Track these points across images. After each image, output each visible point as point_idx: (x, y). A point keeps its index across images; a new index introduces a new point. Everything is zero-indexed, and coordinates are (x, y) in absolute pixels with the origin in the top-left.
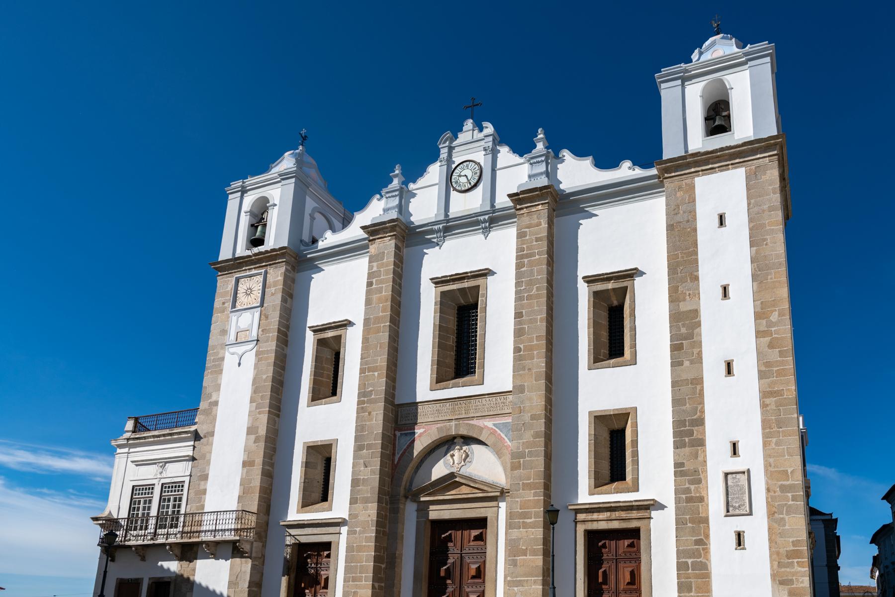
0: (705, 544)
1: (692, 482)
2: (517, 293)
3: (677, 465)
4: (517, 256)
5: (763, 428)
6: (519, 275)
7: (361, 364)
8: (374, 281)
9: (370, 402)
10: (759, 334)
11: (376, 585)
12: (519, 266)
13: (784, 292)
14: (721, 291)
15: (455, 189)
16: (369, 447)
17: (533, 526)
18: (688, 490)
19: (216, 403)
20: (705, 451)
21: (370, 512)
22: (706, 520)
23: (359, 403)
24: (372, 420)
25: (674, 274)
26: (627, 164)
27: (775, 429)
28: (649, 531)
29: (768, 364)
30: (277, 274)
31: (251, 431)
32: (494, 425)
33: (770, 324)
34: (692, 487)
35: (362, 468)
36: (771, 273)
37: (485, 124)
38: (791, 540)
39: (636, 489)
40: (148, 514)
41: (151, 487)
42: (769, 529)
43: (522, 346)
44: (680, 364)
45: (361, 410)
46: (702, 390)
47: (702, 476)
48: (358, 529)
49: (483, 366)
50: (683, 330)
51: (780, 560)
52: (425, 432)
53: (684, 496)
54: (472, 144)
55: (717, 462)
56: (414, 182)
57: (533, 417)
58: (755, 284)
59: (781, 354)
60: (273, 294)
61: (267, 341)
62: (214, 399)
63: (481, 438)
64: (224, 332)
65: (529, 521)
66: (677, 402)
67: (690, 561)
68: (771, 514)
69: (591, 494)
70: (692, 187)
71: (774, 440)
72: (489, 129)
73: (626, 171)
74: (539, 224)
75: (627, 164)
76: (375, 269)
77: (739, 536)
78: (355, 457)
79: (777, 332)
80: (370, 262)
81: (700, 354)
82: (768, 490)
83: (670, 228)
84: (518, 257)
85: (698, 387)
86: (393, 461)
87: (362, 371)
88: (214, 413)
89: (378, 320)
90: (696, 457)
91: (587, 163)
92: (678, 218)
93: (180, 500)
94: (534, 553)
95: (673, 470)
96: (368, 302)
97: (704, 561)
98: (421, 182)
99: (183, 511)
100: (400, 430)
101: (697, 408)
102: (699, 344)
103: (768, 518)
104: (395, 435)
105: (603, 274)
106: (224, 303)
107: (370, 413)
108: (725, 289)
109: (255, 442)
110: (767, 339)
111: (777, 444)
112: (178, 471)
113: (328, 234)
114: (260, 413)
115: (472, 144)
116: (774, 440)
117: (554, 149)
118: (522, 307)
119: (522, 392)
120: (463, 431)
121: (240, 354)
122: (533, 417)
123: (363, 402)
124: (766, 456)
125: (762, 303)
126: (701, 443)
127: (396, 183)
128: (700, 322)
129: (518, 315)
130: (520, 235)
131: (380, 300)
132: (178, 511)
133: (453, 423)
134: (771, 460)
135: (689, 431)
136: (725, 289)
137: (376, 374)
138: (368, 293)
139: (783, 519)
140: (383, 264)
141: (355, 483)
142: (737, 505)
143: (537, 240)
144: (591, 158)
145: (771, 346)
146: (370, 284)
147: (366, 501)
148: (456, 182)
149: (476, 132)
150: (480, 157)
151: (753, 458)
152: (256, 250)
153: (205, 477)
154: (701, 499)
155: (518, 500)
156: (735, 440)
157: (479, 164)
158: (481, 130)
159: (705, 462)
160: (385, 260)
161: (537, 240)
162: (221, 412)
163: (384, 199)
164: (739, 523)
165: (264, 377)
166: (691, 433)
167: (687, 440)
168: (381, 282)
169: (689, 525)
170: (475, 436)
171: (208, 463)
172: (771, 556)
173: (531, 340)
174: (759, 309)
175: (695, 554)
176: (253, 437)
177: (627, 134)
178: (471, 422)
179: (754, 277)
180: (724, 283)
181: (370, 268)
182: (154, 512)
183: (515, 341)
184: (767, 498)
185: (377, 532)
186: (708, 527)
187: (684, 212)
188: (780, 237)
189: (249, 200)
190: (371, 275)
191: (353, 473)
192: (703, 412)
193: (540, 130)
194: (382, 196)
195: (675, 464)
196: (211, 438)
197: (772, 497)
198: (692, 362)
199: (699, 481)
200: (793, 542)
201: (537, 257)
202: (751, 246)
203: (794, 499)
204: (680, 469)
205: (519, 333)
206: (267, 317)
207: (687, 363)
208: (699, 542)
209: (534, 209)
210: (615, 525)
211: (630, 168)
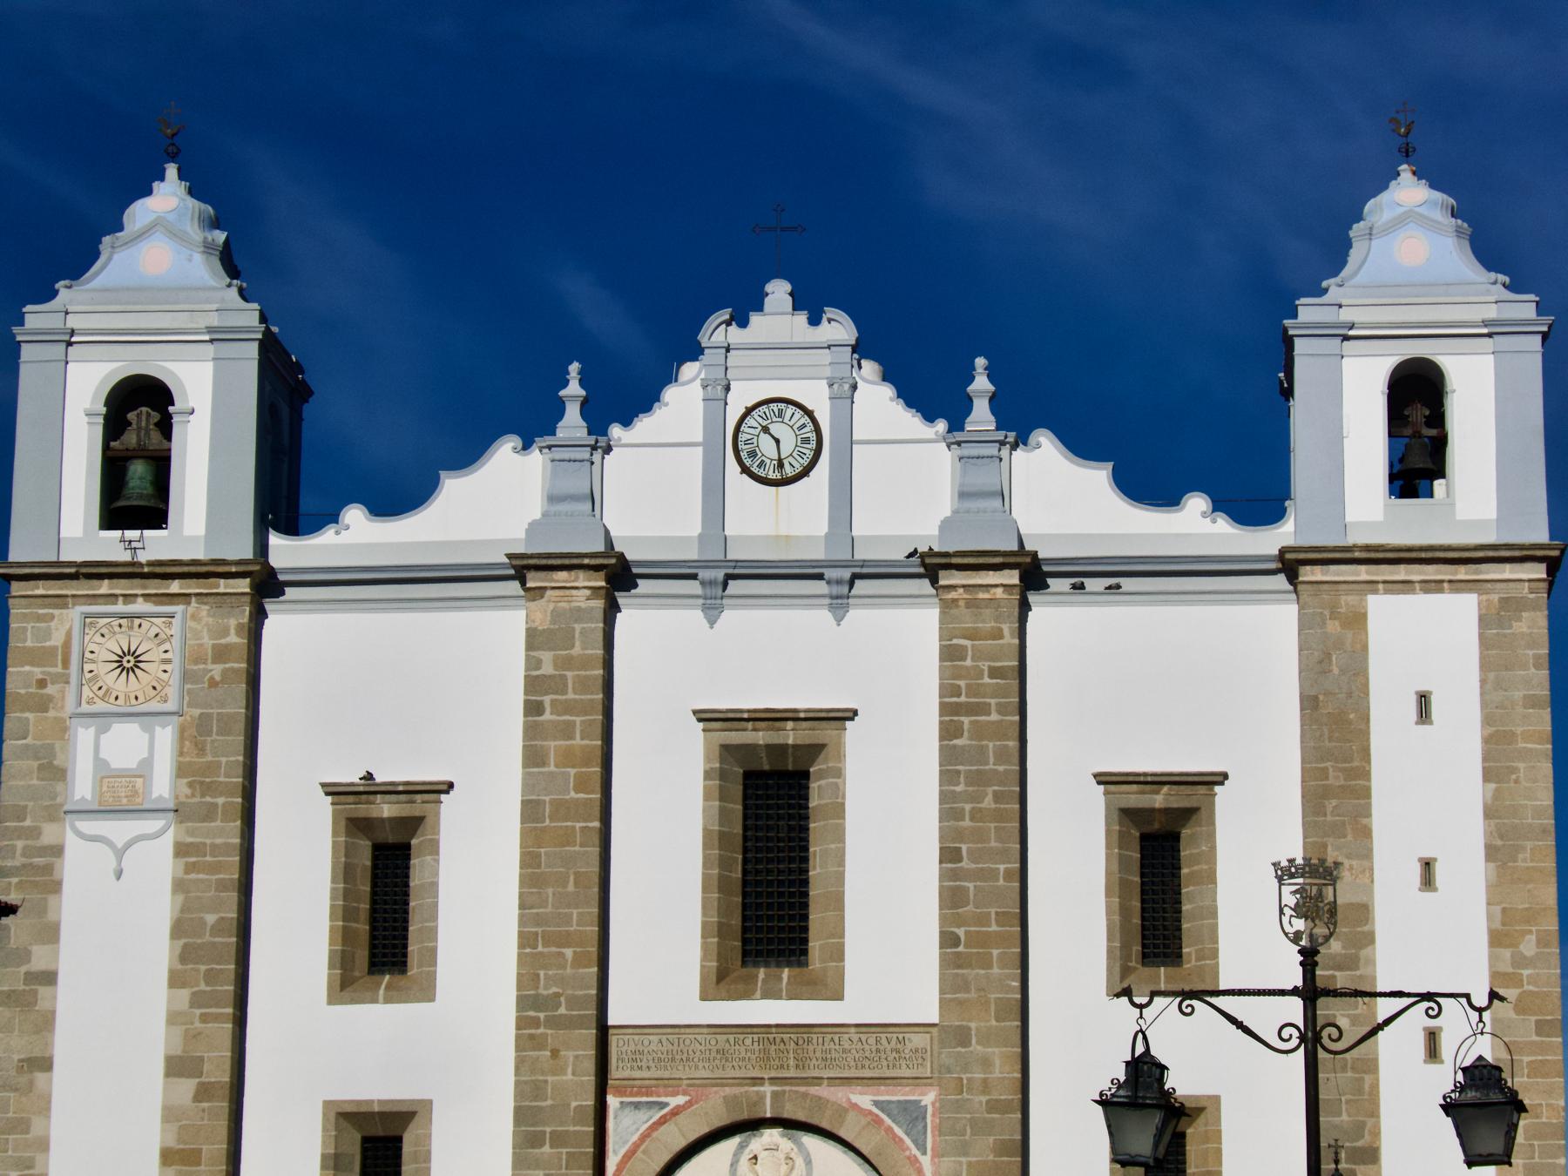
2: (945, 797)
4: (943, 706)
6: (949, 756)
7: (523, 921)
8: (547, 699)
9: (554, 1022)
12: (948, 732)
13: (1548, 894)
14: (1417, 870)
16: (558, 1139)
19: (50, 978)
23: (521, 1023)
24: (563, 1071)
25: (1317, 814)
26: (1197, 503)
31: (176, 1067)
32: (876, 1103)
33: (1520, 961)
36: (1523, 848)
37: (830, 312)
43: (961, 932)
45: (527, 1041)
46: (1375, 1087)
49: (838, 954)
54: (783, 353)
56: (627, 422)
57: (993, 1106)
58: (1492, 865)
59: (1541, 1028)
60: (213, 683)
61: (209, 814)
63: (842, 1134)
72: (839, 329)
73: (1194, 524)
74: (998, 635)
75: (1197, 503)
76: (547, 669)
79: (1532, 980)
83: (1309, 703)
84: (945, 709)
85: (1368, 1078)
87: (525, 940)
88: (42, 1005)
89: (562, 809)
91: (1098, 478)
96: (533, 757)
98: (645, 427)
100: (620, 1092)
105: (1145, 774)
106: (42, 683)
107: (555, 1053)
108: (1427, 865)
109: (198, 1098)
110: (1518, 991)
113: (354, 515)
114: (205, 1018)
115: (783, 353)
117: (1017, 423)
118: (959, 835)
119: (965, 1042)
120: (789, 1112)
121: (120, 845)
122: (993, 1106)
123: (535, 1023)
125: (1504, 910)
127: (572, 424)
129: (949, 855)
131: (567, 758)
133: (767, 1089)
136: (1427, 865)
138: (531, 731)
140: (570, 658)
143: (994, 673)
144: (1110, 465)
146: (533, 708)
149: (802, 318)
150: (815, 395)
152: (155, 545)
157: (809, 413)
158: (814, 321)
160: (577, 650)
161: (994, 673)
162: (71, 1003)
163: (536, 459)
165: (211, 919)
168: (568, 708)
170: (825, 1125)
171: (44, 1145)
173: (983, 920)
174: (1497, 925)
176: (187, 1086)
177: (1200, 425)
178: (813, 1090)
179: (1491, 853)
180: (1427, 854)
181: (532, 663)
183: (943, 919)
187: (1343, 671)
188: (1546, 768)
190: (534, 684)
193: (980, 362)
194: (526, 446)
196: (40, 1077)
201: (994, 717)
202: (1487, 776)
205: (951, 899)
206: (202, 751)
209: (981, 595)
211: (1204, 515)
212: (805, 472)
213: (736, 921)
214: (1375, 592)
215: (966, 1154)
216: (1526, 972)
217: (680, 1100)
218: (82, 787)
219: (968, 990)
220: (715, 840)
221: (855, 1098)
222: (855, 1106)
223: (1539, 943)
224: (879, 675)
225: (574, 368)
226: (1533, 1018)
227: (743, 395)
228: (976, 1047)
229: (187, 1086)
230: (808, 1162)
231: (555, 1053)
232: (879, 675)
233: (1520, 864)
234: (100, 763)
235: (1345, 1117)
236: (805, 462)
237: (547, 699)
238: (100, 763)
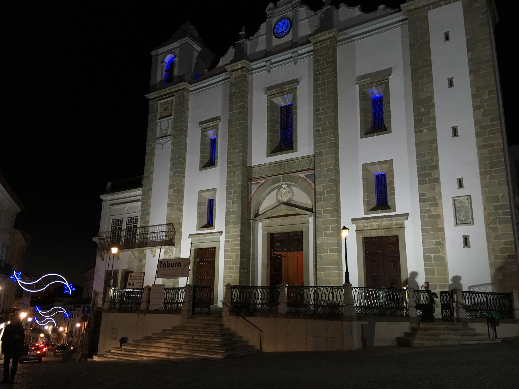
0: (443, 245)
1: (431, 206)
3: (420, 195)
5: (480, 169)
10: (475, 108)
11: (242, 271)
15: (276, 37)
16: (235, 192)
17: (331, 235)
18: (430, 211)
19: (152, 173)
20: (440, 186)
21: (237, 230)
22: (442, 229)
23: (228, 168)
27: (489, 169)
29: (482, 128)
34: (432, 209)
35: (231, 205)
38: (503, 241)
39: (395, 211)
42: (487, 234)
43: (320, 128)
44: (421, 131)
46: (437, 147)
47: (438, 202)
48: (230, 240)
50: (422, 110)
52: (265, 182)
53: (426, 215)
56: (253, 35)
59: (492, 120)
62: (151, 171)
65: (328, 232)
67: (432, 255)
68: (487, 225)
69: (365, 214)
71: (488, 176)
78: (227, 199)
80: (231, 86)
81: (434, 124)
82: (485, 209)
85: (434, 145)
86: (248, 199)
90: (434, 188)
94: (332, 251)
95: (419, 198)
97: (442, 255)
101: (433, 158)
102: (434, 118)
103: (486, 227)
104: (248, 185)
107: (234, 173)
109: (173, 193)
111: (490, 179)
116: (488, 176)
119: (321, 156)
122: (328, 170)
123: (230, 167)
124: (483, 186)
126: (437, 181)
128: (434, 104)
134: (487, 189)
137: (237, 151)
139: (497, 227)
141: (228, 213)
142: (463, 219)
145: (484, 115)
146: (231, 99)
147: (234, 223)
148: (277, 33)
151: (474, 188)
153: (148, 214)
154: (439, 216)
155: (322, 220)
159: (440, 192)
164: (465, 230)
166: (430, 175)
167: (427, 179)
169: (431, 232)
171: (150, 206)
172: (488, 252)
175: (437, 251)
176: (172, 190)
179: (471, 72)
181: (231, 90)
184: (484, 214)
185: (241, 241)
186: (444, 234)
191: (227, 208)
192: (437, 161)
195: (419, 194)
197: (488, 214)
198: (429, 130)
199: (437, 205)
200: (504, 242)
202: (468, 51)
203: (504, 214)
207: (425, 131)
208: (438, 243)
214: (430, 9)
215: (322, 184)
216: (485, 104)
217: (263, 181)
218: (158, 135)
219: (322, 142)
221: (300, 175)
222: (300, 177)
223: (489, 94)
225: (244, 27)
226: (489, 117)
227: (275, 20)
228: (324, 156)
229: (172, 190)
230: (293, 193)
231: (234, 173)
233: (481, 72)
234: (161, 129)
235: (427, 158)
237: (233, 97)
238: (161, 129)
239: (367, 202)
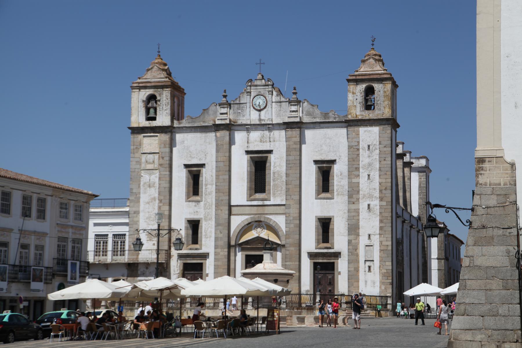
14: (367, 177)
15: (254, 108)
28: (338, 263)
30: (165, 137)
40: (106, 249)
41: (107, 235)
51: (383, 275)
55: (363, 240)
64: (139, 163)
66: (349, 219)
69: (316, 249)
70: (359, 132)
77: (369, 267)
92: (353, 144)
93: (124, 242)
99: (127, 248)
112: (123, 229)
130: (287, 139)
132: (124, 248)
135: (353, 229)
141: (216, 239)
151: (376, 240)
156: (370, 233)
182: (110, 247)
189: (144, 94)
204: (350, 242)
210: (325, 261)
212: (265, 108)
213: (254, 186)
220: (249, 173)
224: (278, 144)
232: (278, 144)
236: (264, 106)
239: (318, 242)
